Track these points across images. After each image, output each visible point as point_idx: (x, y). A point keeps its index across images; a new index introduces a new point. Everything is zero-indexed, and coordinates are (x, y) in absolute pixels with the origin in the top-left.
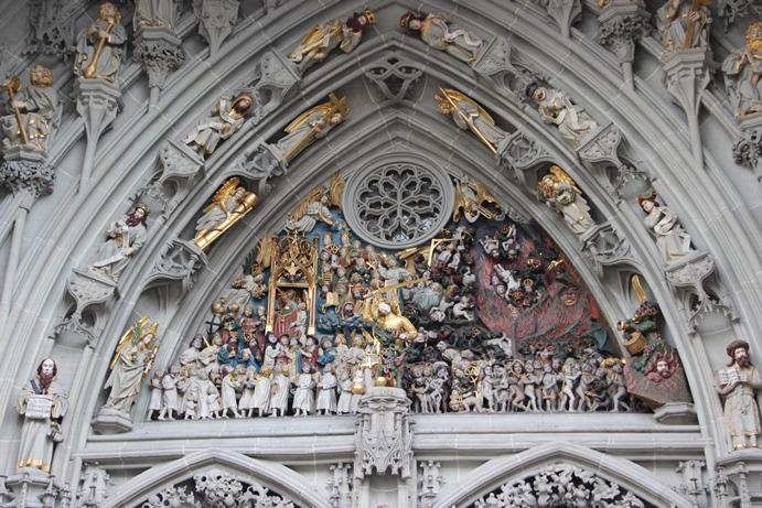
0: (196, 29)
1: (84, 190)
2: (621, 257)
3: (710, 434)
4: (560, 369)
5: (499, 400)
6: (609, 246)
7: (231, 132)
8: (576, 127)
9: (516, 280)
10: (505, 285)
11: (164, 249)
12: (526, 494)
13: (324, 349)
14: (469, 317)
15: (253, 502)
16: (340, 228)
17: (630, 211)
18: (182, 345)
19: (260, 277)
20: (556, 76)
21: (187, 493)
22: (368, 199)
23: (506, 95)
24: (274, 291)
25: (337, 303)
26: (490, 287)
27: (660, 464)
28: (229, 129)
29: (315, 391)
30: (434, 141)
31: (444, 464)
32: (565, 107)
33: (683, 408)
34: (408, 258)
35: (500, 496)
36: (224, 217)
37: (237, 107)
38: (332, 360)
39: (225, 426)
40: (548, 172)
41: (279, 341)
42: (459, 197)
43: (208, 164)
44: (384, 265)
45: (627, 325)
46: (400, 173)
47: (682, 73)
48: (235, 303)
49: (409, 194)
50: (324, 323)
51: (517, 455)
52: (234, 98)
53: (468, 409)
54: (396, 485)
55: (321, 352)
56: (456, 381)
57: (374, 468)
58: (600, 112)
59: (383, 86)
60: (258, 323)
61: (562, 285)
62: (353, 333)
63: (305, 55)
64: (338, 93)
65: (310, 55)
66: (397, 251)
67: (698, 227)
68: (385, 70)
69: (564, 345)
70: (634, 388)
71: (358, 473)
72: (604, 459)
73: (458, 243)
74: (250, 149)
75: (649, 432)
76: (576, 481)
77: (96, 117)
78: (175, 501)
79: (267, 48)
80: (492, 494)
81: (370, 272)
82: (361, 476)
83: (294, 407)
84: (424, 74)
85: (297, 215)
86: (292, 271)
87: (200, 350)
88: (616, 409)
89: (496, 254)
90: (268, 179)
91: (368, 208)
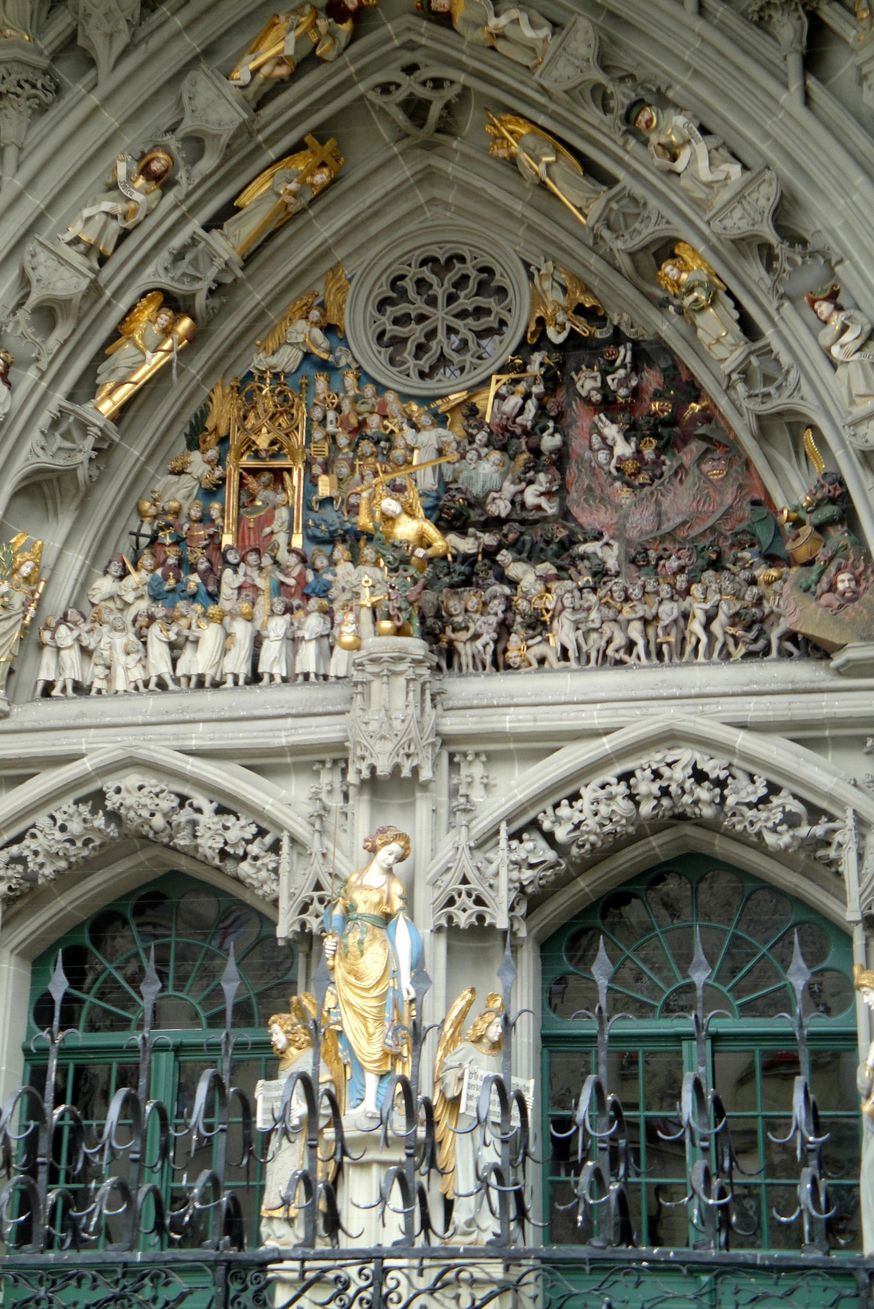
0: (74, 36)
2: (784, 399)
4: (687, 592)
5: (585, 648)
7: (140, 216)
9: (627, 439)
10: (611, 449)
11: (44, 420)
12: (619, 799)
13: (316, 570)
14: (551, 508)
16: (343, 363)
18: (89, 573)
19: (213, 453)
21: (94, 812)
22: (389, 309)
23: (595, 122)
24: (235, 477)
25: (335, 493)
26: (588, 454)
27: (840, 743)
28: (135, 211)
30: (492, 203)
31: (491, 758)
32: (689, 142)
34: (452, 410)
35: (577, 805)
37: (146, 171)
40: (674, 256)
41: (243, 559)
42: (537, 299)
43: (108, 270)
44: (414, 426)
45: (794, 515)
46: (442, 261)
48: (175, 500)
50: (317, 526)
51: (605, 739)
52: (143, 155)
53: (535, 665)
54: (413, 794)
55: (310, 576)
56: (519, 619)
57: (373, 769)
58: (752, 145)
59: (400, 117)
60: (211, 531)
61: (704, 445)
62: (362, 543)
63: (255, 72)
64: (321, 133)
65: (265, 71)
66: (435, 398)
68: (398, 86)
69: (703, 549)
71: (352, 777)
72: (741, 739)
74: (177, 242)
75: (821, 691)
76: (699, 776)
78: (75, 827)
79: (193, 63)
80: (565, 802)
83: (261, 670)
84: (465, 88)
85: (271, 345)
86: (262, 442)
87: (121, 578)
89: (596, 397)
90: (211, 292)
91: (389, 327)
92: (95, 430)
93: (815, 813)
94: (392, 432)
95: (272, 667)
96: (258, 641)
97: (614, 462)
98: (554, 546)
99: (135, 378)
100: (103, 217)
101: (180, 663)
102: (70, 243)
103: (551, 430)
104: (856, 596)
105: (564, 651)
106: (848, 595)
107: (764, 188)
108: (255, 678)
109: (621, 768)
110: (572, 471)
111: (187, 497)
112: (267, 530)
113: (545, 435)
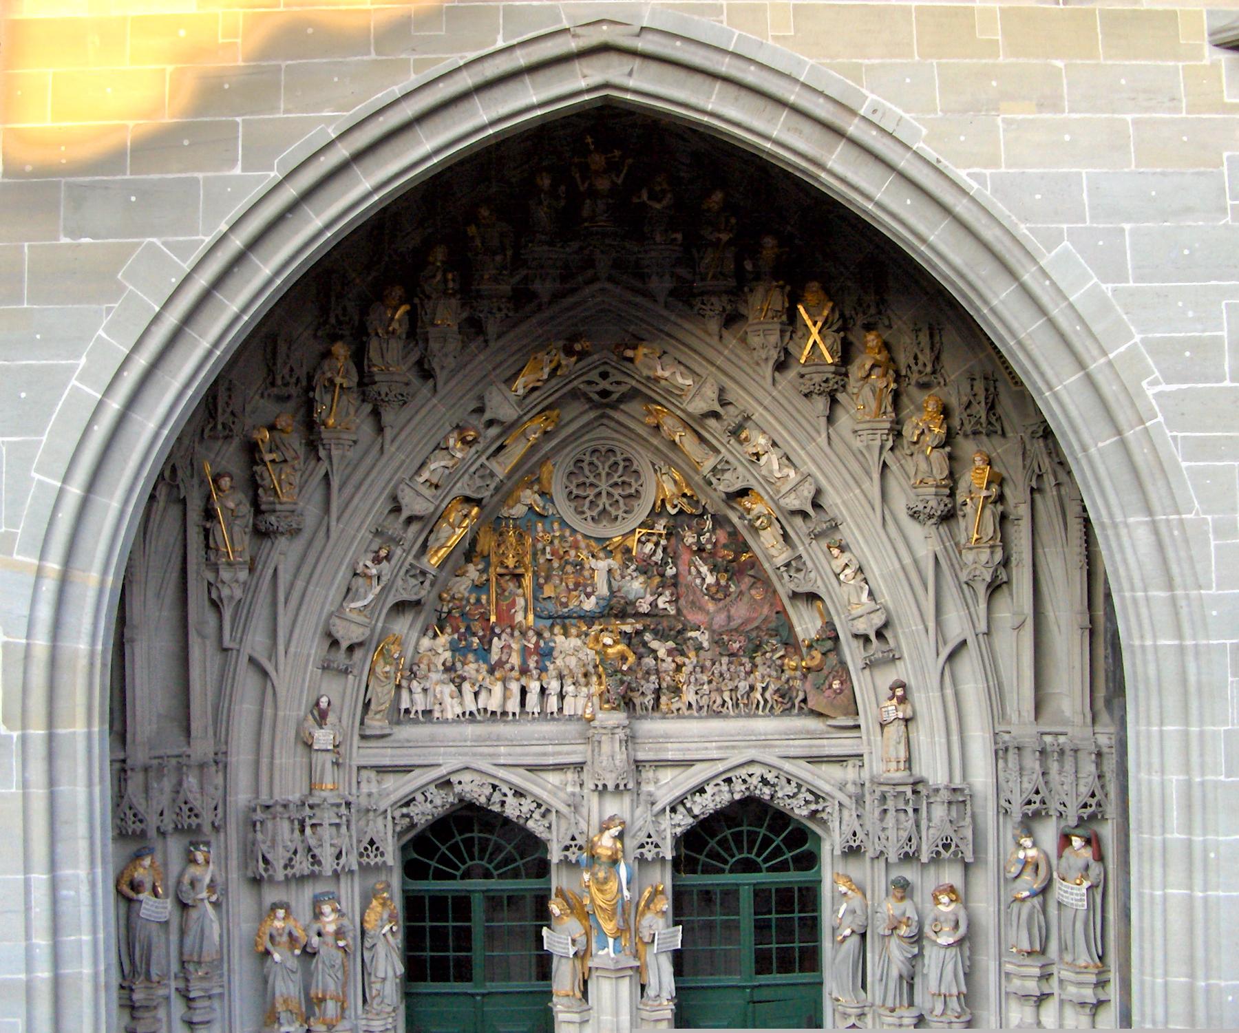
1: (333, 535)
3: (869, 743)
6: (798, 570)
8: (779, 475)
15: (503, 803)
17: (819, 548)
19: (480, 567)
20: (758, 413)
25: (553, 595)
33: (851, 723)
35: (705, 796)
36: (453, 535)
37: (464, 441)
38: (552, 649)
39: (470, 730)
44: (593, 556)
47: (870, 437)
59: (596, 397)
61: (753, 580)
67: (875, 571)
72: (787, 766)
73: (660, 535)
74: (472, 469)
76: (764, 781)
77: (335, 461)
81: (581, 564)
82: (593, 787)
84: (633, 388)
85: (511, 502)
86: (511, 562)
93: (817, 797)
96: (524, 692)
98: (672, 633)
105: (690, 705)
107: (807, 484)
109: (724, 777)
110: (682, 590)
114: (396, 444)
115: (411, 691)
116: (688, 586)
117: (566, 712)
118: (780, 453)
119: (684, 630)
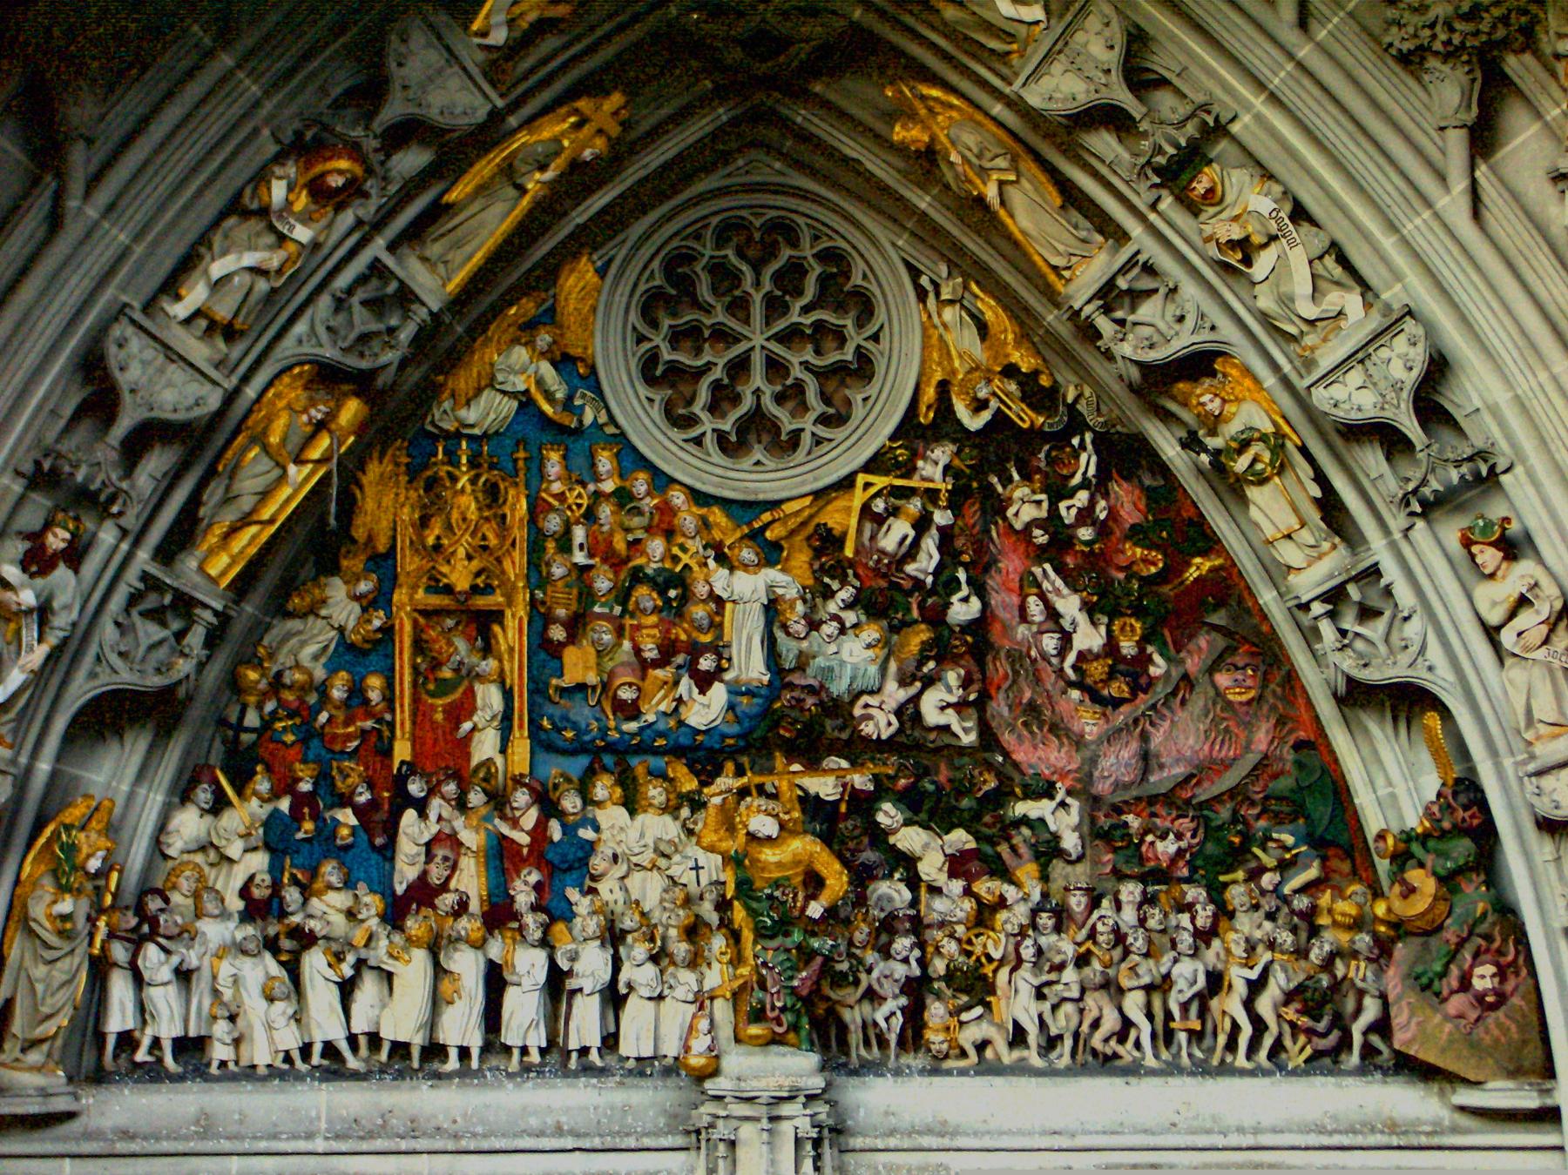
6: (1367, 613)
8: (1310, 312)
9: (1094, 623)
10: (1066, 639)
19: (364, 587)
24: (408, 627)
25: (592, 678)
29: (557, 985)
33: (1529, 1100)
34: (792, 533)
38: (590, 847)
41: (432, 791)
44: (722, 559)
49: (786, 309)
61: (1221, 642)
69: (1220, 828)
70: (1409, 1042)
73: (932, 495)
81: (681, 581)
84: (855, 27)
88: (1354, 1059)
89: (1040, 537)
92: (208, 616)
94: (686, 566)
95: (525, 1038)
96: (496, 981)
97: (1071, 658)
99: (266, 514)
100: (247, 278)
101: (356, 1009)
102: (187, 322)
103: (965, 591)
104: (1502, 998)
106: (1490, 999)
107: (1400, 343)
108: (493, 1044)
110: (1000, 668)
111: (316, 657)
112: (467, 726)
113: (955, 599)
114: (103, 196)
115: (139, 980)
116: (1017, 657)
117: (627, 1047)
118: (1319, 243)
119: (1000, 797)
